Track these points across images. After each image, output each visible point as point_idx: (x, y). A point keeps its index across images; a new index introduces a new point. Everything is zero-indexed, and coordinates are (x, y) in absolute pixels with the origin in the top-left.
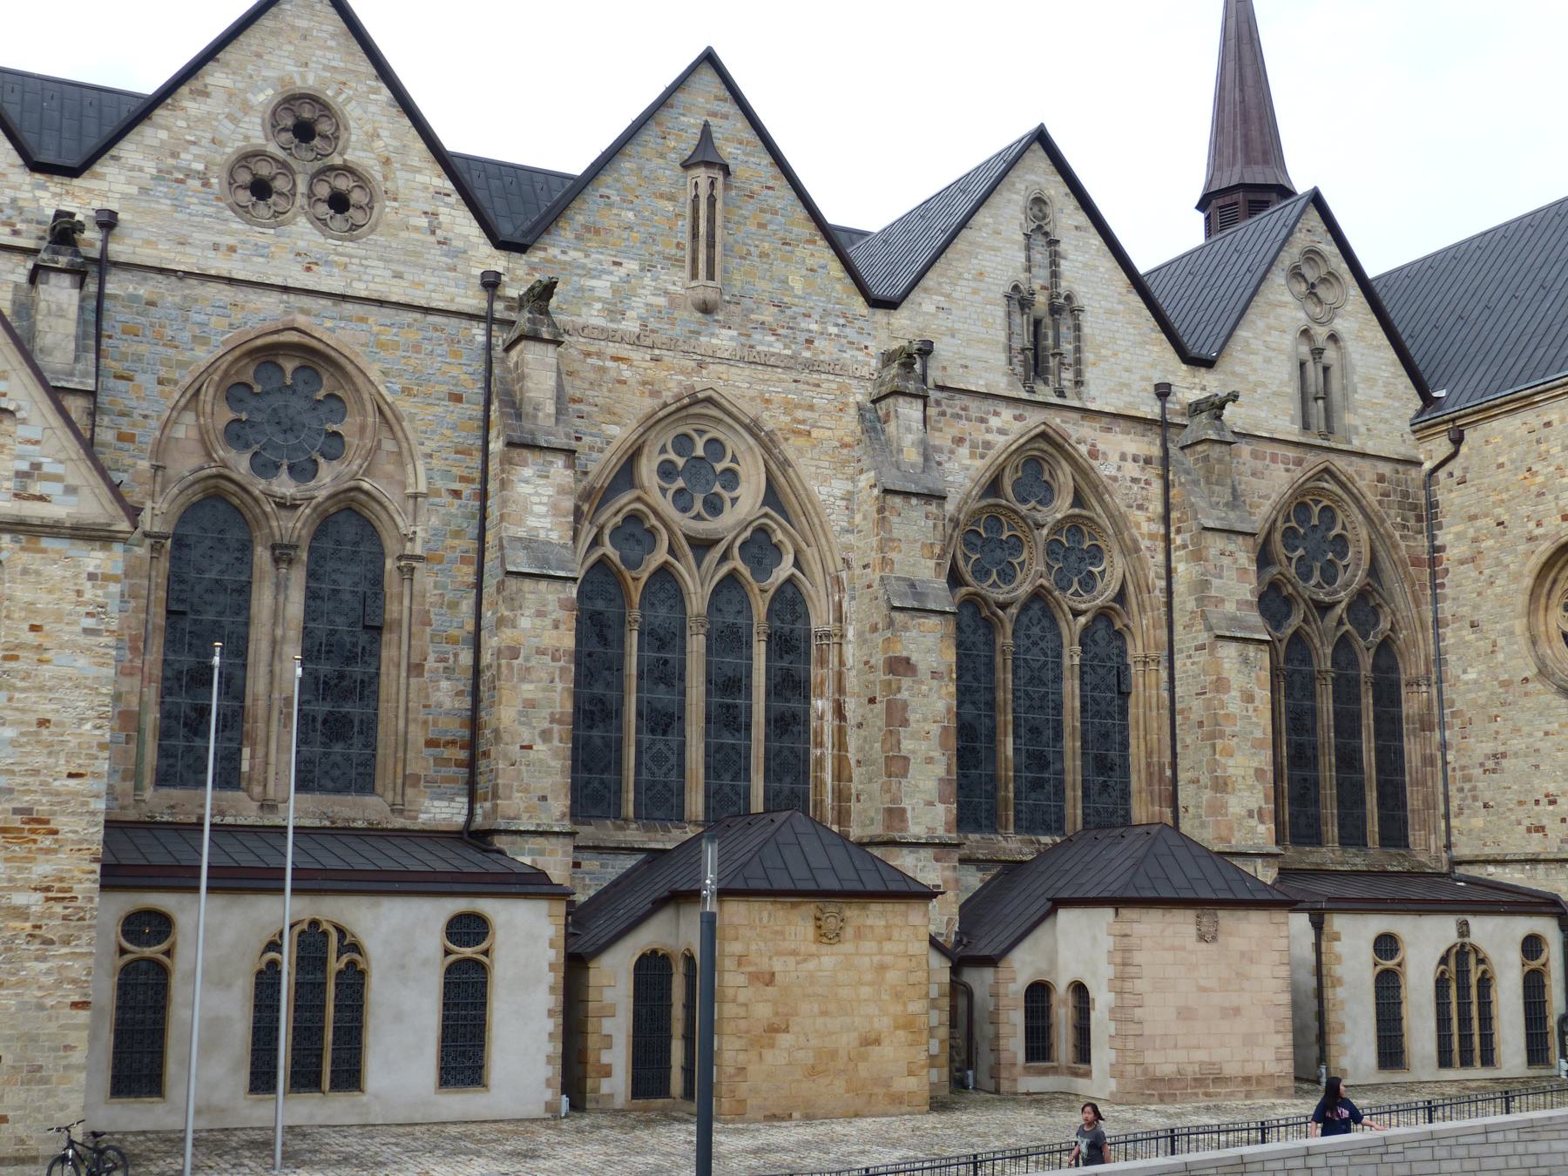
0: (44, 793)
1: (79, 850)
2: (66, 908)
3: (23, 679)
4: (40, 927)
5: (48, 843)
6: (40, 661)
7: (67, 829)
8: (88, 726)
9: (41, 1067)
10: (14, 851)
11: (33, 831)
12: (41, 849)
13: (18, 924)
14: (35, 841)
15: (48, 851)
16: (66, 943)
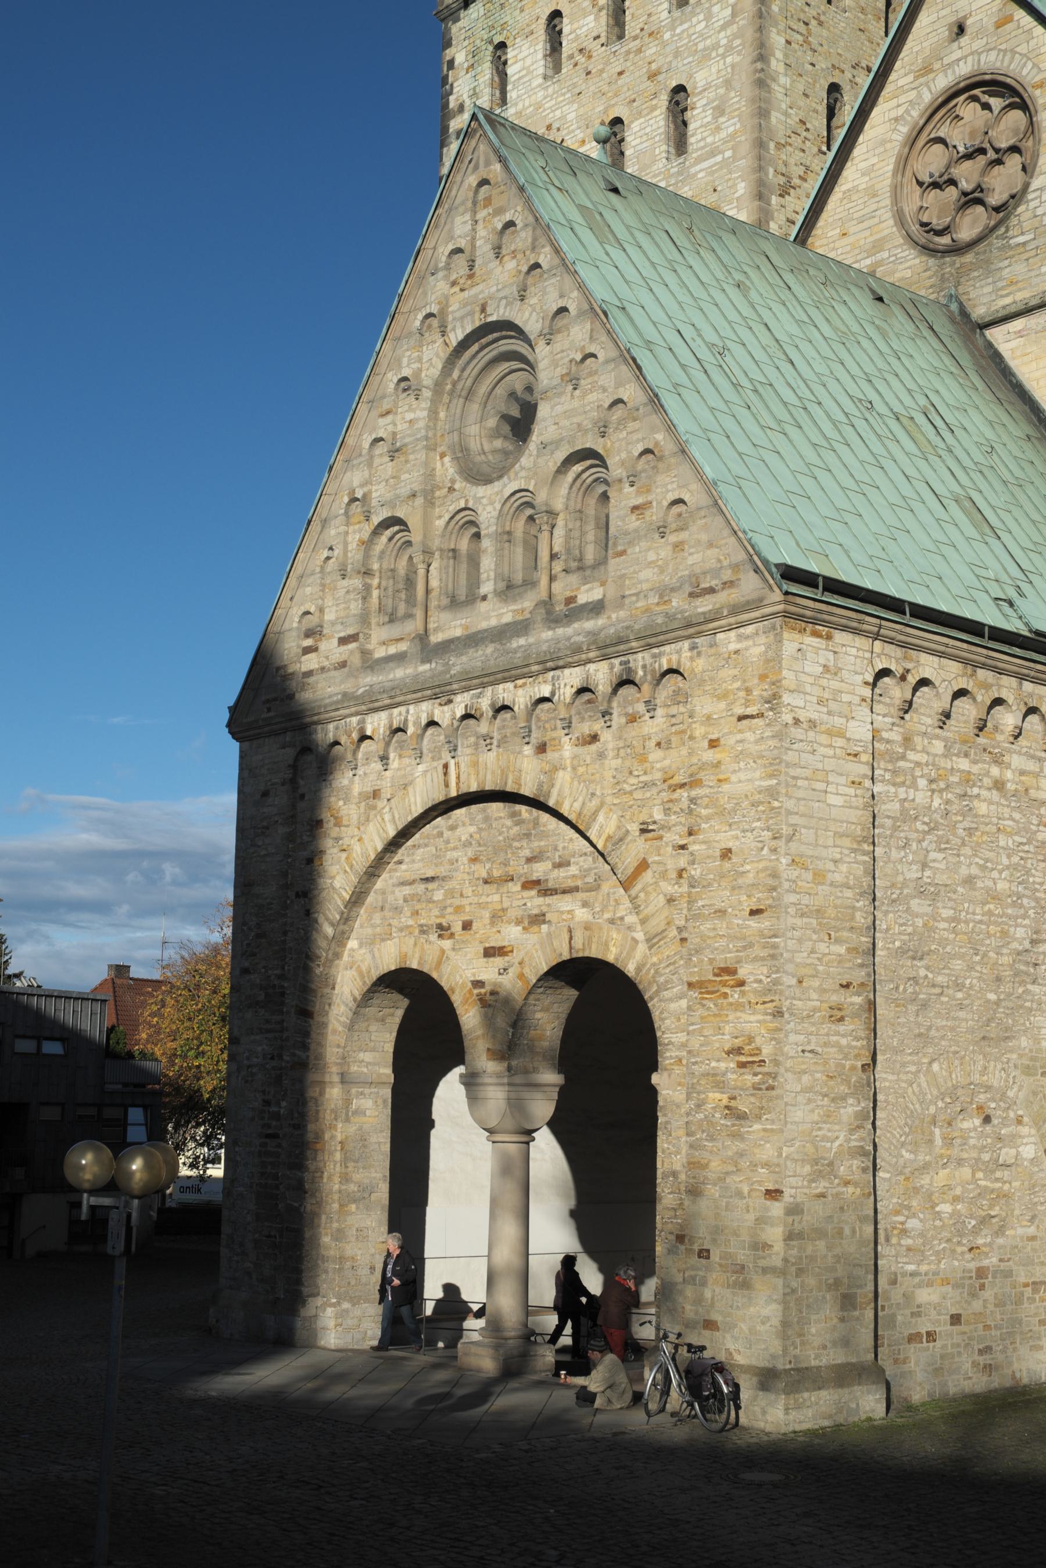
0: (732, 938)
1: (764, 1003)
2: (756, 1074)
3: (707, 807)
4: (733, 1098)
5: (736, 996)
6: (720, 781)
7: (752, 978)
8: (765, 851)
9: (743, 1267)
10: (709, 1009)
11: (724, 984)
12: (731, 1004)
13: (718, 1096)
14: (725, 995)
15: (737, 1007)
16: (759, 1117)
